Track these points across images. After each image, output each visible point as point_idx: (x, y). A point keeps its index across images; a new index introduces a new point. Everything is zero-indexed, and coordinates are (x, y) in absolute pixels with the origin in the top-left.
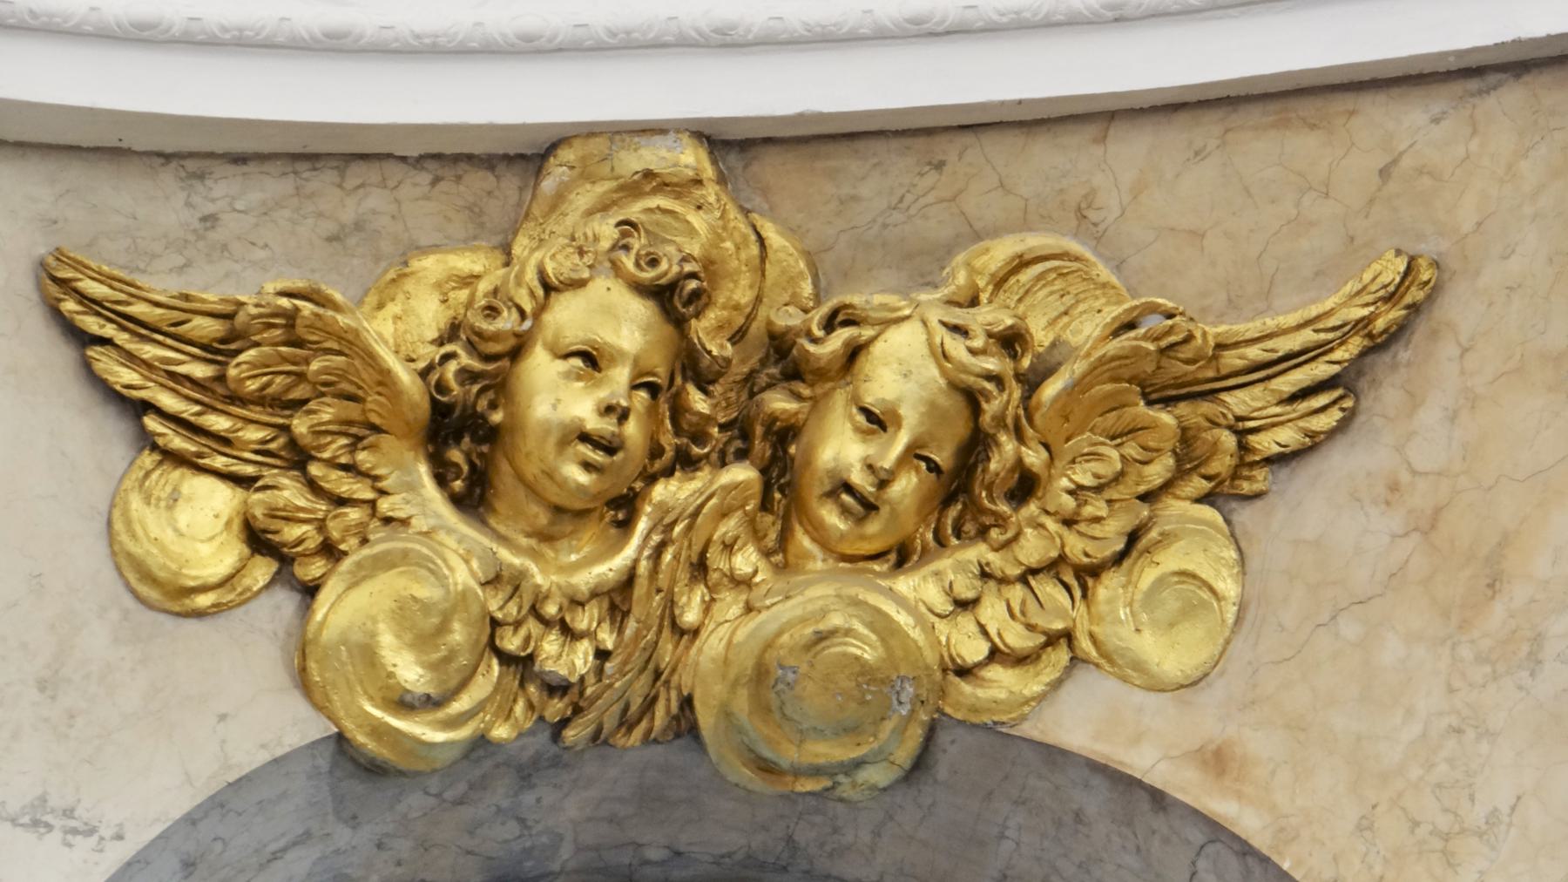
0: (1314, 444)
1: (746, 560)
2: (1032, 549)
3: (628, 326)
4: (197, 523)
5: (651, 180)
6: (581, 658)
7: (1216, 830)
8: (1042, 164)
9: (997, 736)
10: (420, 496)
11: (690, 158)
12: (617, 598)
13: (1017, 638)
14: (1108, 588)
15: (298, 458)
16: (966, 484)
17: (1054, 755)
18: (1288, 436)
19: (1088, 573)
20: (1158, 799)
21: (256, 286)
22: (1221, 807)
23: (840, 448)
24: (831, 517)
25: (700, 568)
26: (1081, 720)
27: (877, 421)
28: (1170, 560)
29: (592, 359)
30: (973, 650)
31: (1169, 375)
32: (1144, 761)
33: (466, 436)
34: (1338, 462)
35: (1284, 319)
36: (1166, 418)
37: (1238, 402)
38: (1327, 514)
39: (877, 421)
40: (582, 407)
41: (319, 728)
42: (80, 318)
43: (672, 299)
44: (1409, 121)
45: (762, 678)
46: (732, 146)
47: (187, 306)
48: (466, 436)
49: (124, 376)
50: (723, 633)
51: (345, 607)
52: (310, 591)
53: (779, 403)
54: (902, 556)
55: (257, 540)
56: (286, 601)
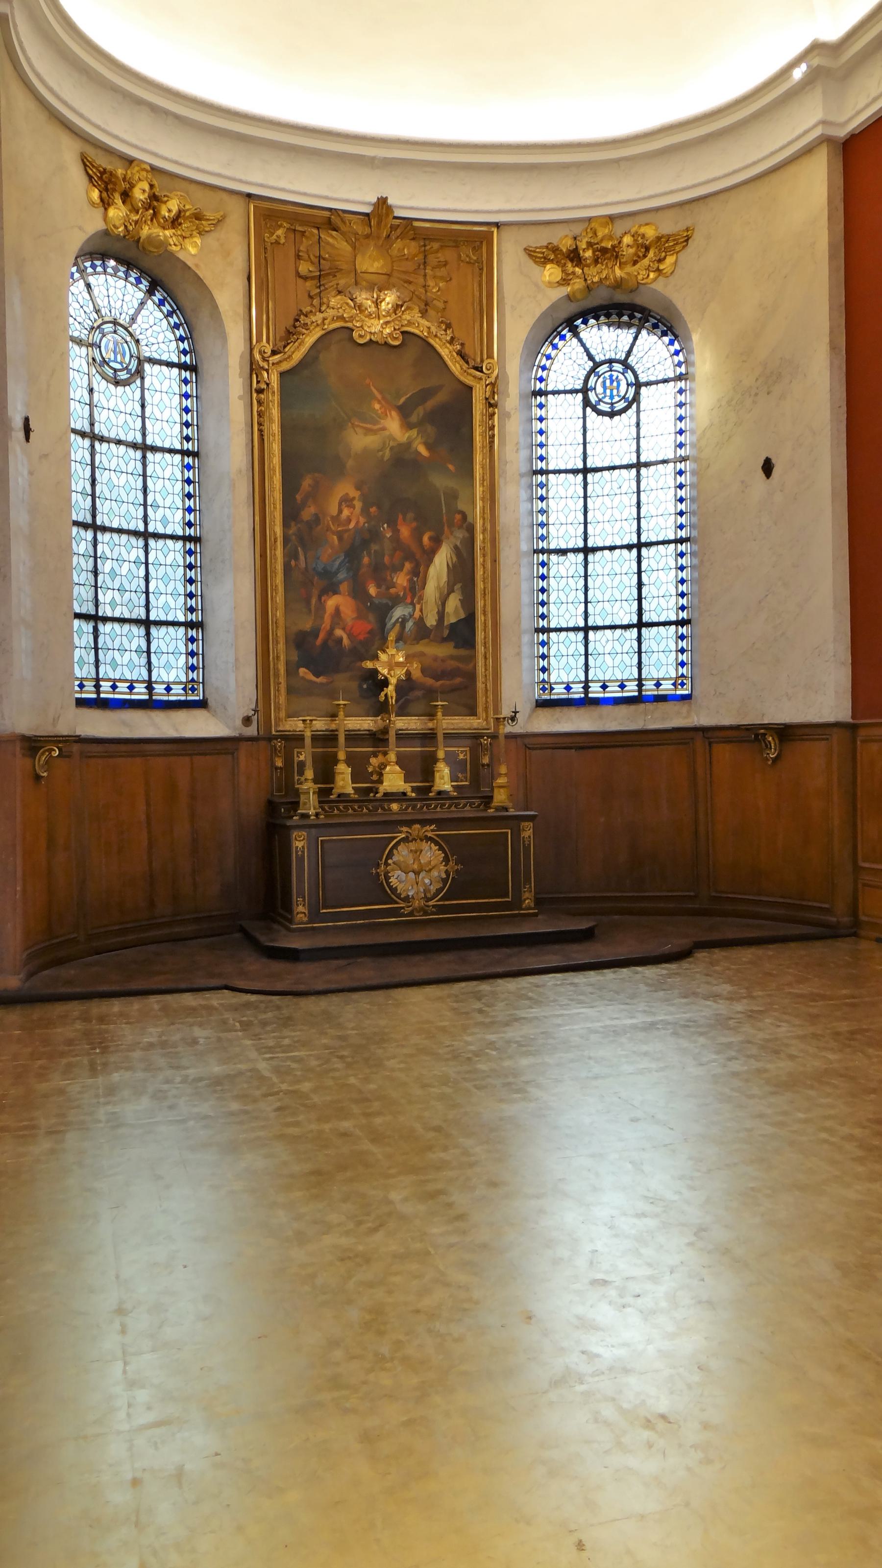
0: (211, 230)
1: (149, 222)
2: (179, 233)
3: (147, 187)
4: (95, 194)
5: (144, 170)
6: (131, 228)
7: (196, 275)
8: (185, 185)
9: (172, 255)
10: (118, 201)
11: (148, 168)
12: (136, 222)
13: (177, 243)
14: (187, 240)
15: (107, 190)
16: (175, 222)
17: (178, 259)
18: (207, 229)
19: (184, 238)
20: (189, 268)
21: (109, 167)
22: (197, 272)
23: (164, 212)
24: (162, 221)
25: (145, 222)
26: (181, 256)
27: (170, 211)
28: (195, 239)
29: (144, 191)
30: (172, 243)
31: (198, 217)
32: (189, 263)
33: (126, 196)
34: (213, 234)
35: (209, 214)
36: (197, 222)
37: (203, 222)
38: (211, 239)
39: (170, 211)
40: (142, 197)
41: (105, 227)
42: (85, 163)
43: (152, 186)
44: (225, 196)
45: (149, 237)
46: (154, 169)
47: (100, 166)
48: (126, 196)
49: (90, 172)
50: (145, 231)
51: (112, 212)
52: (106, 209)
53: (155, 203)
54: (164, 228)
55: (102, 200)
56: (102, 209)
